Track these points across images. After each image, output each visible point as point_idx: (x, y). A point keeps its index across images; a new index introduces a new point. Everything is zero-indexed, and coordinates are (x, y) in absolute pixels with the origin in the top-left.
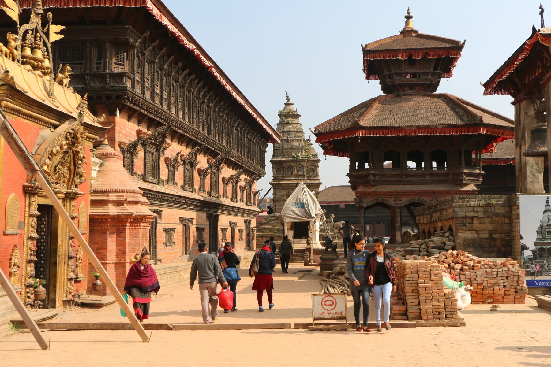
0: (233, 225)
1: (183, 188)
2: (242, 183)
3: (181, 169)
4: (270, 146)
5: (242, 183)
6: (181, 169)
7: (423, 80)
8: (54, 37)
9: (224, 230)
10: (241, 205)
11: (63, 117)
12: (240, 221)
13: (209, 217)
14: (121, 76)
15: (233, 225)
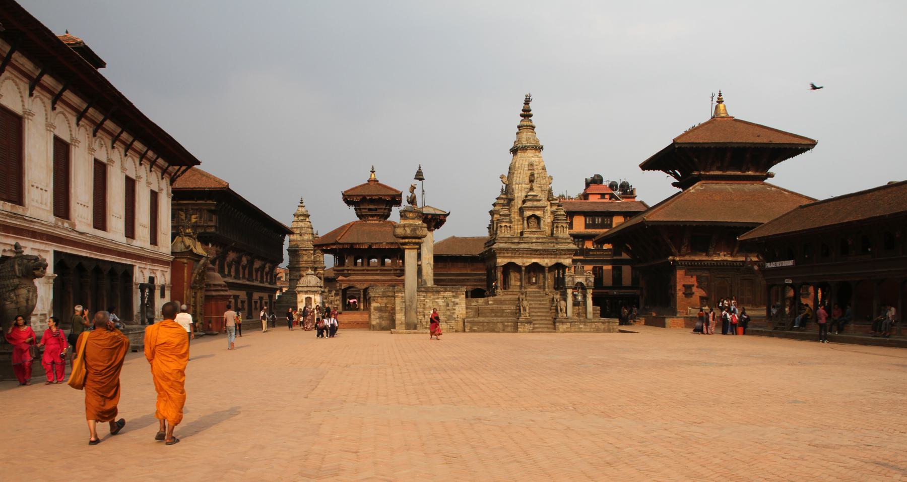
0: (261, 298)
1: (235, 278)
2: (267, 269)
3: (234, 267)
4: (287, 238)
5: (267, 269)
6: (234, 267)
7: (380, 212)
8: (194, 220)
9: (256, 302)
10: (267, 285)
11: (201, 257)
12: (265, 296)
13: (247, 294)
14: (211, 226)
15: (261, 298)
